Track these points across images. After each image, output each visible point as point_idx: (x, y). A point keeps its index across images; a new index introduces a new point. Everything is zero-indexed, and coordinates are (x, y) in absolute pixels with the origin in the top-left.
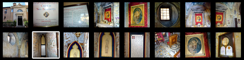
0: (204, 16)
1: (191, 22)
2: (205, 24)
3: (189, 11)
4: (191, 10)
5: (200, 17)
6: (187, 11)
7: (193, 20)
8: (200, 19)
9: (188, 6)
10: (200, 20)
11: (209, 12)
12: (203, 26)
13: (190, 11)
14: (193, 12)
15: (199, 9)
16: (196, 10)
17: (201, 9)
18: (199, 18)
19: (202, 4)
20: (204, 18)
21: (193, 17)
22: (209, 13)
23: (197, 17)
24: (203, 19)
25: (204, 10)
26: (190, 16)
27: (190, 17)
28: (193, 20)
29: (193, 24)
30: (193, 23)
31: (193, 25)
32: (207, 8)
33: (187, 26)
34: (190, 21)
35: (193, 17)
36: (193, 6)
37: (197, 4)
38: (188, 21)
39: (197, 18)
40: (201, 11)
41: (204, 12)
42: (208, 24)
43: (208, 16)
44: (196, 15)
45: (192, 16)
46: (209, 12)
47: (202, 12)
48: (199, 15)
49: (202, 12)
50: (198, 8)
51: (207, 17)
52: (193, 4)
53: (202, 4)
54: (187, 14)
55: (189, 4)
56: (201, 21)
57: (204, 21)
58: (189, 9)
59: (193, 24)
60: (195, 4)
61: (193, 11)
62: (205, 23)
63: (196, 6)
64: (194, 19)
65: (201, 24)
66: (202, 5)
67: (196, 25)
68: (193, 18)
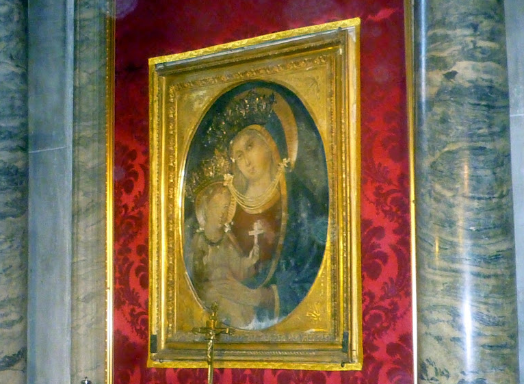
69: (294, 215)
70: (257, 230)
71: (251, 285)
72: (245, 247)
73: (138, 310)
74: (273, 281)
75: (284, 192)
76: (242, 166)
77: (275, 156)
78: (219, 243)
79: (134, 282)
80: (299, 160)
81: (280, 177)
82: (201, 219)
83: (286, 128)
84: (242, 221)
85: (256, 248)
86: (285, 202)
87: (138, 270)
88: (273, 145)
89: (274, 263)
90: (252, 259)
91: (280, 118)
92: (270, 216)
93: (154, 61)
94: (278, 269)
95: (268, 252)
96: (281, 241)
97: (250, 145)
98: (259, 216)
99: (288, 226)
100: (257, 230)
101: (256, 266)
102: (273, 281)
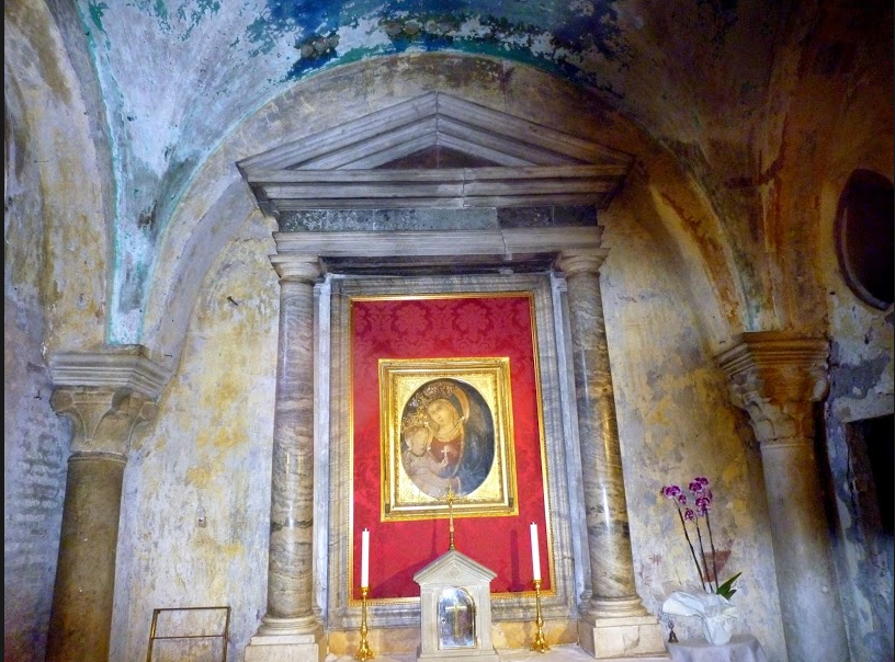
0: (593, 363)
1: (238, 521)
2: (612, 564)
3: (181, 229)
4: (230, 200)
5: (489, 381)
6: (149, 222)
7: (294, 458)
8: (488, 442)
9: (170, 104)
10: (474, 461)
11: (715, 264)
12: (555, 627)
13: (217, 227)
14: (297, 267)
15: (460, 189)
16: (385, 212)
17: (515, 166)
18: (446, 422)
19: (541, 45)
20: (595, 403)
21: (308, 388)
22: (702, 282)
23: (407, 378)
24: (547, 443)
25: (583, 214)
26: (203, 372)
27: (228, 390)
28: (294, 458)
29: (290, 583)
30: (291, 537)
31: (290, 599)
32: (676, 161)
33: (139, 626)
34: (219, 507)
35: (295, 388)
36: (284, 109)
37: (401, 39)
38: (159, 506)
39: (391, 433)
40: (509, 219)
41: (578, 263)
42: (689, 573)
43: (698, 356)
44: (386, 349)
45: (268, 352)
46: (707, 245)
47: (540, 264)
48: (445, 347)
49: (540, 264)
50: (421, 159)
51: (672, 384)
52: (287, 48)
53: (541, 45)
54: (134, 301)
55: (200, 48)
56: (494, 491)
57: (591, 510)
58: (178, 171)
59: (290, 583)
60: (348, 38)
61: (287, 219)
62: (609, 540)
63: (376, 99)
64: (332, 433)
65: (512, 579)
66: (522, 72)
67: (366, 614)
68: (307, 416)
69: (468, 444)
70: (446, 450)
71: (443, 477)
72: (439, 459)
73: (372, 491)
74: (457, 474)
75: (462, 432)
76: (435, 417)
77: (457, 417)
78: (422, 455)
79: (368, 474)
80: (470, 418)
81: (460, 426)
82: (408, 443)
83: (462, 402)
84: (436, 446)
85: (446, 458)
86: (463, 437)
87: (372, 470)
88: (454, 410)
89: (457, 466)
90: (444, 463)
91: (457, 396)
92: (455, 443)
93: (380, 361)
94: (460, 469)
95: (453, 460)
96: (461, 456)
97: (439, 409)
98: (446, 443)
99: (465, 448)
100: (446, 450)
101: (446, 468)
102: (457, 474)
